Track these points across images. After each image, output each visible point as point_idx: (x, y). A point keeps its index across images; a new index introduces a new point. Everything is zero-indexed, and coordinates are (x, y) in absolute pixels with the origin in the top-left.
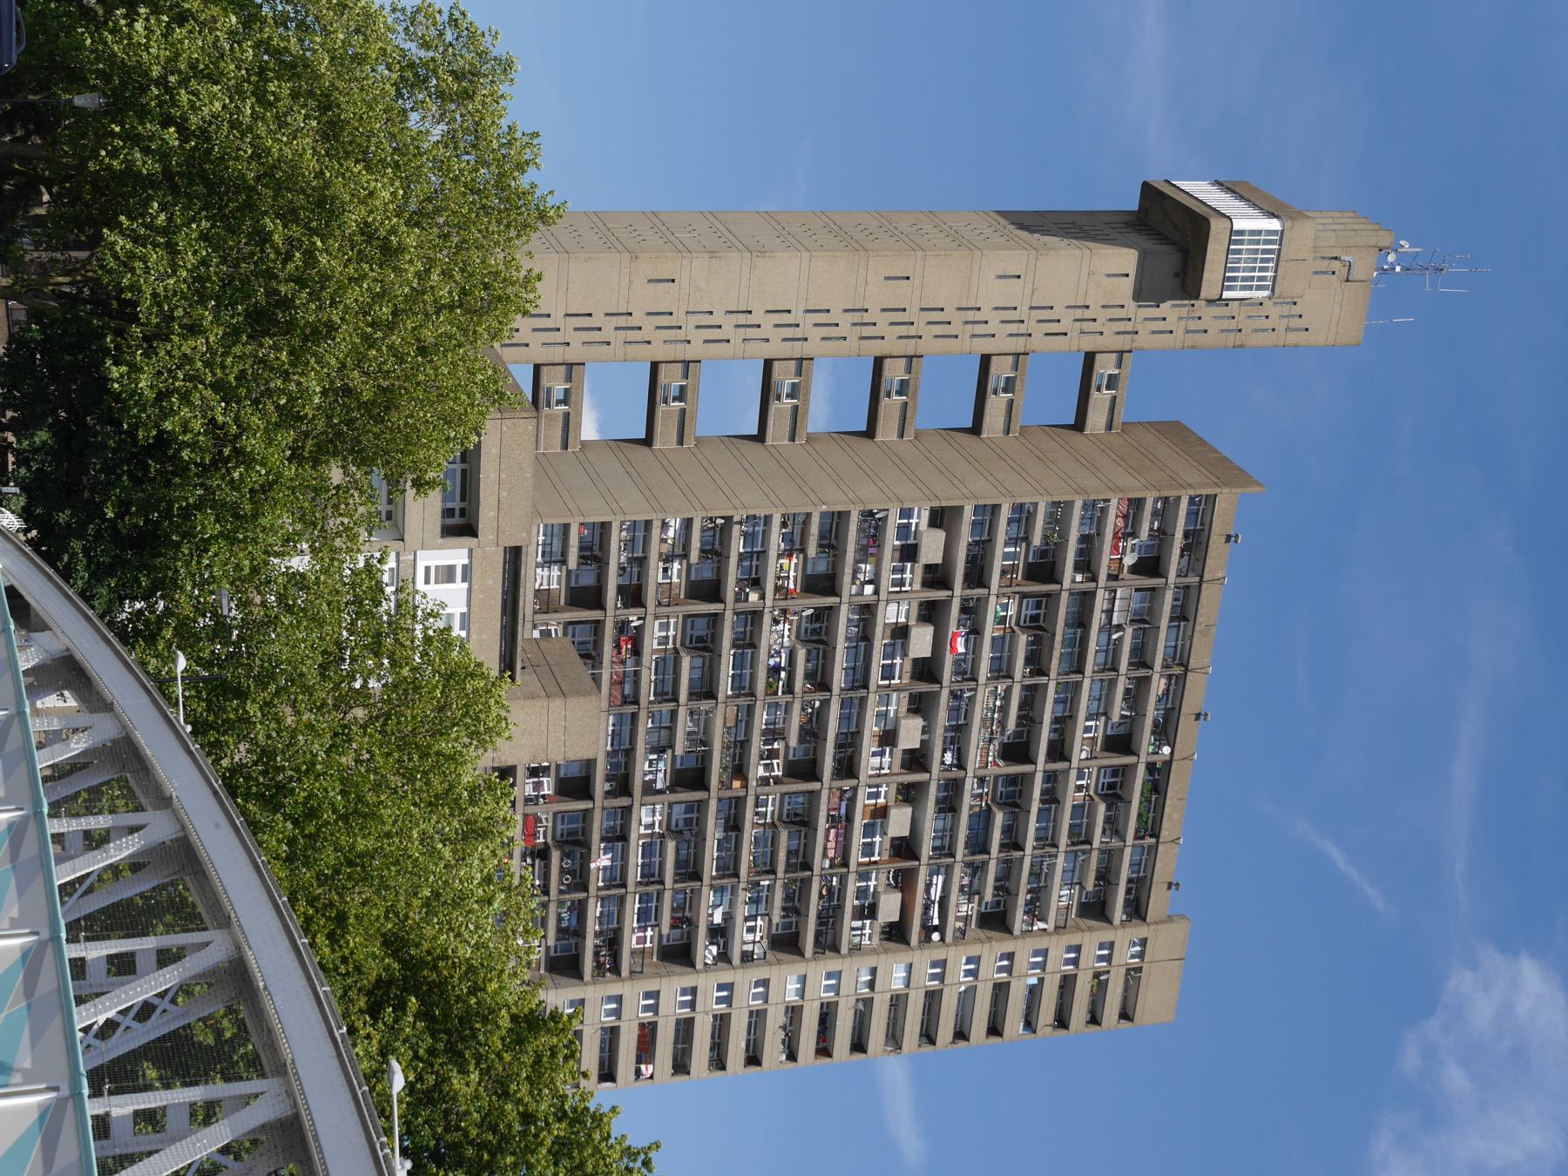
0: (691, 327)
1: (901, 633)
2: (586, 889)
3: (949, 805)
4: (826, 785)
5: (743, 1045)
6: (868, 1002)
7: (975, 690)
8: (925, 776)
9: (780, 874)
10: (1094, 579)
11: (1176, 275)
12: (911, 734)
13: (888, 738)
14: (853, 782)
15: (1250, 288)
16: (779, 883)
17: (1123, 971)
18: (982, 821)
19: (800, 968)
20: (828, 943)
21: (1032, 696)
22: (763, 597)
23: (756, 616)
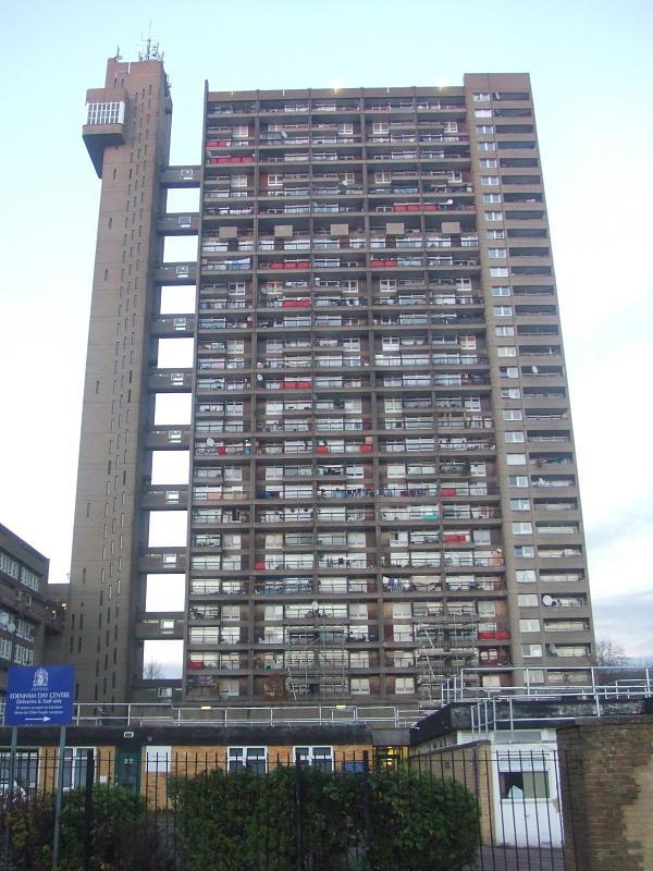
1: (280, 242)
4: (368, 269)
8: (367, 219)
12: (343, 229)
15: (117, 113)
20: (475, 255)
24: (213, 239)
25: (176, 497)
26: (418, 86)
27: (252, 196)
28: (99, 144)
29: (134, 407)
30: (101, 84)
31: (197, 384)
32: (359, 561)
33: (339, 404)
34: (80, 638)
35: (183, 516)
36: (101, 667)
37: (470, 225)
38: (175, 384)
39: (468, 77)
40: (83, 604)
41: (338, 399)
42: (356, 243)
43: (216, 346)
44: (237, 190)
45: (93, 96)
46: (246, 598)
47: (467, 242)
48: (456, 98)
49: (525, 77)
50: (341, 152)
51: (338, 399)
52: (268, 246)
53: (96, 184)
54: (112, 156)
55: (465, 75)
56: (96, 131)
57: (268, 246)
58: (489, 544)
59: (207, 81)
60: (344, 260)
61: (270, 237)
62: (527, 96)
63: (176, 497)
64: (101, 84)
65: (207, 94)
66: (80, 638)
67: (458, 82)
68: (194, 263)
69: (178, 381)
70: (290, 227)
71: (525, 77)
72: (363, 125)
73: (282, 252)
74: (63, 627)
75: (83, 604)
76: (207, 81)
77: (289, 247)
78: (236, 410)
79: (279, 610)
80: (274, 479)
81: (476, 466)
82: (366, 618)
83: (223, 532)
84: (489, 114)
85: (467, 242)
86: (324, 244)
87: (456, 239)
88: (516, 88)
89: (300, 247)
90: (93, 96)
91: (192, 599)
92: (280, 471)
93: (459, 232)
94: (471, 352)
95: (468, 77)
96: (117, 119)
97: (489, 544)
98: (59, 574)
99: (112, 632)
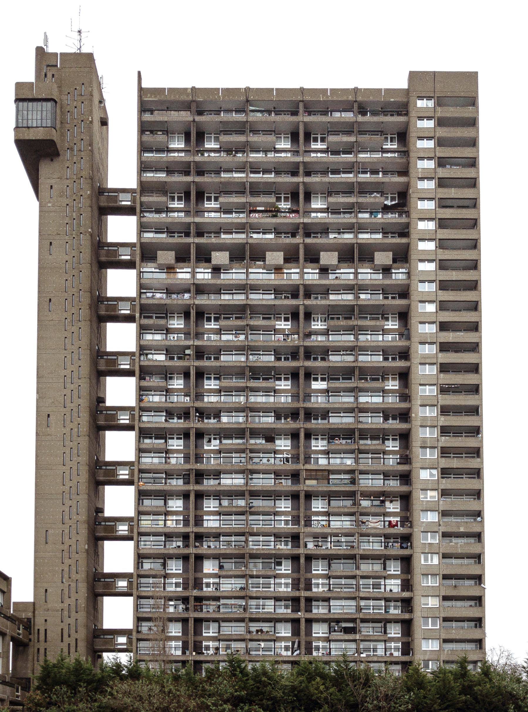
1: (216, 270)
8: (301, 247)
13: (278, 270)
25: (126, 528)
26: (362, 86)
27: (190, 216)
28: (36, 153)
29: (84, 442)
31: (140, 416)
32: (284, 587)
33: (270, 439)
34: (46, 649)
35: (130, 545)
37: (402, 256)
38: (122, 422)
39: (413, 76)
41: (270, 436)
43: (155, 381)
44: (173, 210)
47: (399, 275)
48: (397, 105)
49: (471, 78)
50: (277, 169)
51: (270, 436)
52: (204, 275)
53: (32, 205)
54: (46, 170)
55: (411, 73)
56: (31, 135)
57: (204, 275)
60: (277, 291)
61: (207, 264)
62: (472, 101)
64: (30, 77)
65: (141, 90)
67: (401, 83)
68: (135, 298)
69: (124, 419)
70: (227, 254)
71: (471, 78)
72: (300, 137)
73: (219, 282)
74: (30, 640)
81: (391, 502)
83: (165, 558)
85: (399, 275)
86: (258, 274)
87: (386, 270)
88: (461, 90)
89: (234, 276)
91: (140, 615)
94: (392, 391)
95: (413, 76)
98: (23, 591)
99: (73, 644)
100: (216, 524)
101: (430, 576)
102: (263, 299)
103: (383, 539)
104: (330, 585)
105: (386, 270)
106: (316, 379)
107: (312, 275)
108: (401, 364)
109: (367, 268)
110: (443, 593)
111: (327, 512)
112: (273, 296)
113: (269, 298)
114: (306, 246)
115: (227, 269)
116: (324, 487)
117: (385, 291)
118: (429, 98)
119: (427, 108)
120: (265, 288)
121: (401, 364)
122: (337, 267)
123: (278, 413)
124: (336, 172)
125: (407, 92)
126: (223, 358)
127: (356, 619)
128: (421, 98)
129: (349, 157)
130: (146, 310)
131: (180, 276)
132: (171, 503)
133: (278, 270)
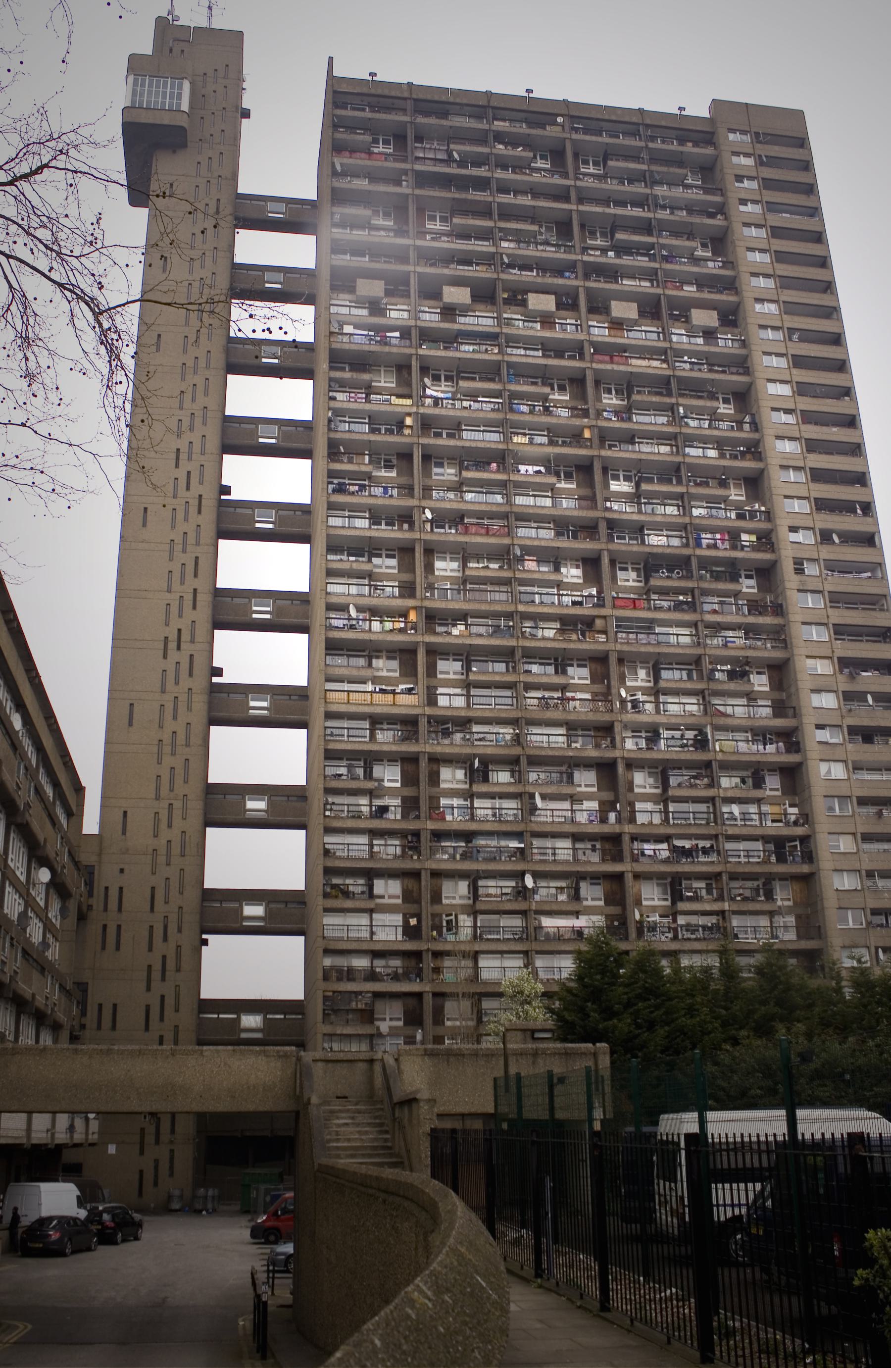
0: (188, 494)
2: (688, 558)
3: (612, 274)
4: (589, 365)
5: (835, 429)
6: (791, 331)
7: (501, 254)
8: (581, 290)
9: (673, 400)
10: (405, 172)
11: (174, 152)
13: (547, 321)
14: (586, 345)
16: (681, 401)
17: (758, 146)
18: (622, 249)
19: (760, 383)
21: (507, 213)
22: (409, 414)
23: (426, 424)
24: (347, 296)
26: (647, 107)
30: (146, 47)
36: (156, 975)
37: (731, 318)
40: (122, 871)
42: (567, 329)
44: (378, 228)
45: (136, 64)
46: (417, 866)
58: (779, 793)
59: (331, 59)
62: (802, 142)
63: (265, 704)
65: (331, 78)
66: (119, 927)
75: (122, 871)
76: (331, 59)
77: (467, 322)
78: (387, 565)
79: (463, 887)
80: (451, 676)
82: (399, 901)
84: (749, 162)
90: (136, 64)
92: (457, 666)
93: (717, 325)
96: (179, 105)
97: (779, 793)
100: (460, 702)
101: (836, 800)
102: (526, 356)
103: (749, 735)
104: (666, 812)
105: (709, 334)
106: (616, 478)
107: (600, 332)
108: (748, 464)
109: (680, 328)
110: (861, 829)
111: (651, 688)
112: (540, 353)
113: (536, 357)
114: (588, 290)
115: (464, 310)
116: (643, 643)
117: (711, 361)
118: (744, 132)
119: (742, 142)
120: (528, 343)
121: (748, 464)
122: (635, 323)
123: (561, 525)
124: (622, 204)
125: (711, 121)
126: (465, 434)
127: (718, 875)
128: (733, 131)
129: (640, 189)
130: (337, 359)
131: (394, 314)
132: (378, 663)
133: (547, 321)
